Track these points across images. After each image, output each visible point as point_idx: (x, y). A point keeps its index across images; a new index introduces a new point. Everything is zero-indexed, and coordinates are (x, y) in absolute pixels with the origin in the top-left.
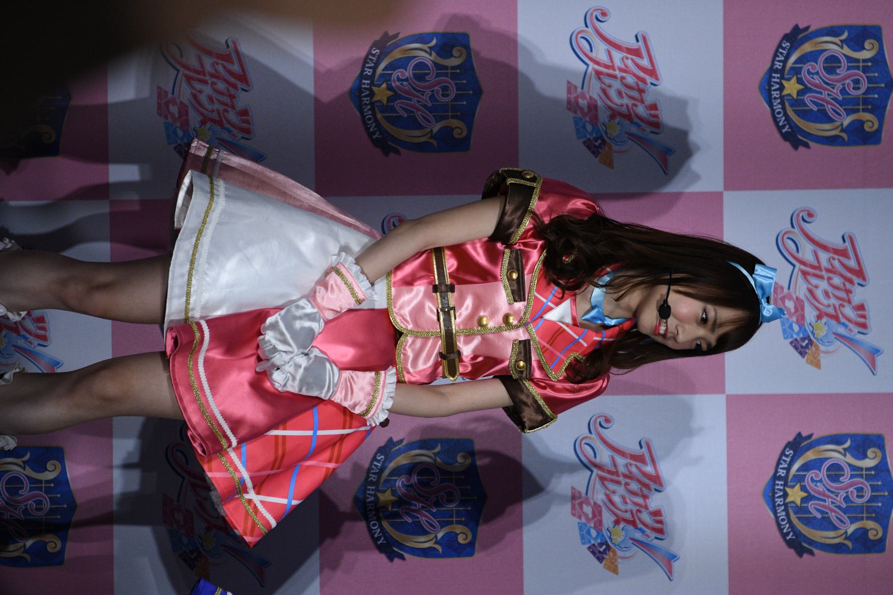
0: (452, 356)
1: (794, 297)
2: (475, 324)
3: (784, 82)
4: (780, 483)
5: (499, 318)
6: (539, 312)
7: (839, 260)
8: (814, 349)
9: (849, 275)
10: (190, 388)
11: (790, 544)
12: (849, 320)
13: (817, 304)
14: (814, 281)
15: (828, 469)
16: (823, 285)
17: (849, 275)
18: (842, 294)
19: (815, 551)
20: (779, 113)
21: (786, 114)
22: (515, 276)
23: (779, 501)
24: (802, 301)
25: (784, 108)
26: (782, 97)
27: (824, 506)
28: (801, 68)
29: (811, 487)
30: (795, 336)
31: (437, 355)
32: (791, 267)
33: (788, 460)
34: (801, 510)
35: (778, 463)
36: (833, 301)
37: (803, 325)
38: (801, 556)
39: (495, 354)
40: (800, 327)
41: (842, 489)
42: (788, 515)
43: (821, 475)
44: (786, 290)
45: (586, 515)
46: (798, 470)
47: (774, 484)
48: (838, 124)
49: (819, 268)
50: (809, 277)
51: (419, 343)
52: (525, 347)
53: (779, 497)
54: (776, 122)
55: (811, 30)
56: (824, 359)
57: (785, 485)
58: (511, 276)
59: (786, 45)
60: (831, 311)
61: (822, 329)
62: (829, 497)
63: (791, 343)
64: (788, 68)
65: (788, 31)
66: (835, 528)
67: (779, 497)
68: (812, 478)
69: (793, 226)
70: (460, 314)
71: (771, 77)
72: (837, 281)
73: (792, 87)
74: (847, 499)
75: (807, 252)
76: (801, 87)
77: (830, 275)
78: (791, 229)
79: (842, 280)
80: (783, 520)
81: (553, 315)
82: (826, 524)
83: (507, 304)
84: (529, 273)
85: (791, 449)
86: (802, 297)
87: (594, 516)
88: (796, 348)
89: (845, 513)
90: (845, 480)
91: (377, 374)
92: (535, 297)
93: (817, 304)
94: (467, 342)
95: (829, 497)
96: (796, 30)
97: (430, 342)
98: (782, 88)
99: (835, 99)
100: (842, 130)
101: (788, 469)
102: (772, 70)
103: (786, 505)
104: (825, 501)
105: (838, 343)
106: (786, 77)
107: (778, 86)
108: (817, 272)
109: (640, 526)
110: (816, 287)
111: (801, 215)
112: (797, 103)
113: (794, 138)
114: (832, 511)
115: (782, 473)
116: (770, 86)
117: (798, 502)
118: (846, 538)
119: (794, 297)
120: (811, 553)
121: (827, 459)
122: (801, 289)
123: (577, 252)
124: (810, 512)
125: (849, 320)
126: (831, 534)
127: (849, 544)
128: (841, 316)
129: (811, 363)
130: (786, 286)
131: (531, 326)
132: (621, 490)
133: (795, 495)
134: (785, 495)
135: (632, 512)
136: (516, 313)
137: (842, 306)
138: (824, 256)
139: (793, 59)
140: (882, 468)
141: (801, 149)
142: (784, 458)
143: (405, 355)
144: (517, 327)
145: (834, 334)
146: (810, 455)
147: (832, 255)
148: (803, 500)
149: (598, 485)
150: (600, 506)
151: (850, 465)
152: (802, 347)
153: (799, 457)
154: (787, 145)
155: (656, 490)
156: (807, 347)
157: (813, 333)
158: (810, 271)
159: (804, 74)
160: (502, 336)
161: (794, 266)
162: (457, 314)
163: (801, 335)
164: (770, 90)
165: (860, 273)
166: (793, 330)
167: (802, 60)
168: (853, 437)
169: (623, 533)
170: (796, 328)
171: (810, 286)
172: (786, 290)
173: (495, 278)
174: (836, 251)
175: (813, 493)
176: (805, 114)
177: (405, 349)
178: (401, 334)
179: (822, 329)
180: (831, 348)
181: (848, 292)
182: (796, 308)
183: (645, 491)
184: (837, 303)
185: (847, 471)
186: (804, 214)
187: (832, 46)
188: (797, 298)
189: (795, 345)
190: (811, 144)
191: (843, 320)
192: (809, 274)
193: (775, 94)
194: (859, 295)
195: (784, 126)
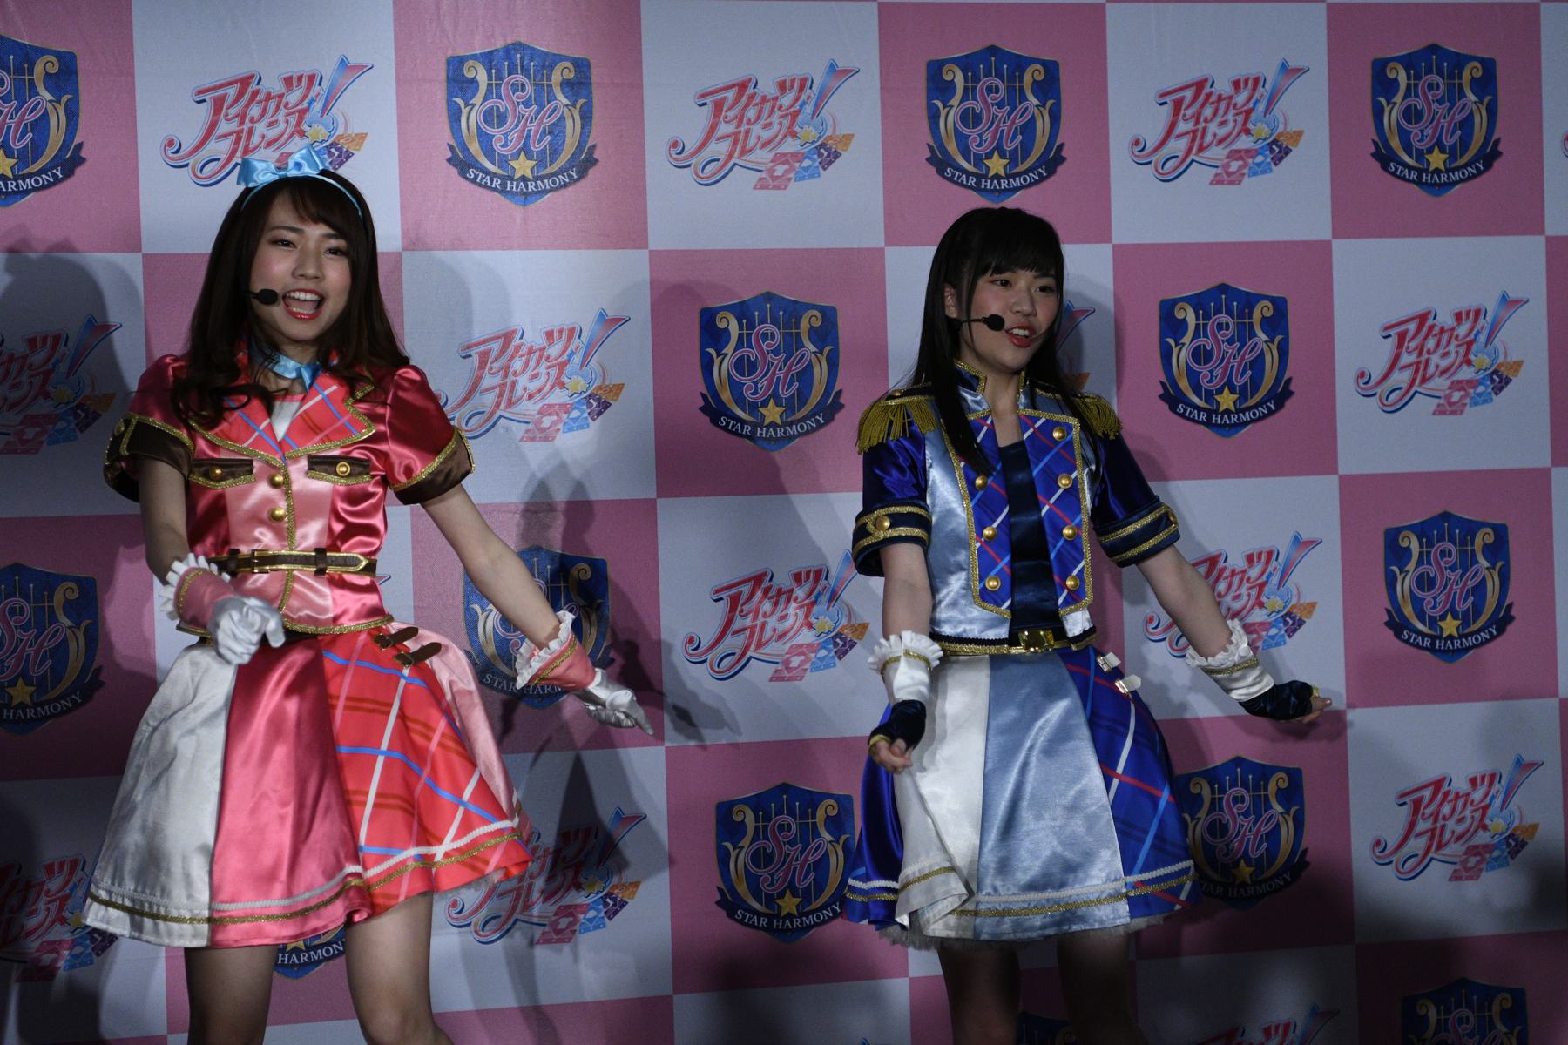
9: (744, 99)
14: (752, 141)
17: (744, 99)
21: (555, 174)
25: (548, 176)
26: (536, 179)
34: (1013, 160)
35: (961, 185)
38: (1064, 159)
42: (1019, 174)
44: (764, 175)
46: (969, 161)
47: (985, 190)
55: (452, 143)
56: (842, 130)
64: (500, 172)
65: (454, 171)
71: (511, 192)
72: (751, 113)
73: (523, 166)
74: (1000, 105)
75: (718, 149)
90: (978, 106)
99: (538, 112)
101: (968, 174)
102: (503, 191)
103: (1008, 177)
112: (541, 163)
134: (997, 177)
140: (966, 64)
164: (525, 194)
165: (742, 86)
167: (489, 153)
168: (930, 98)
172: (764, 175)
176: (555, 152)
179: (809, 132)
184: (777, 113)
186: (674, 152)
187: (472, 119)
193: (531, 187)
194: (767, 87)
195: (570, 176)
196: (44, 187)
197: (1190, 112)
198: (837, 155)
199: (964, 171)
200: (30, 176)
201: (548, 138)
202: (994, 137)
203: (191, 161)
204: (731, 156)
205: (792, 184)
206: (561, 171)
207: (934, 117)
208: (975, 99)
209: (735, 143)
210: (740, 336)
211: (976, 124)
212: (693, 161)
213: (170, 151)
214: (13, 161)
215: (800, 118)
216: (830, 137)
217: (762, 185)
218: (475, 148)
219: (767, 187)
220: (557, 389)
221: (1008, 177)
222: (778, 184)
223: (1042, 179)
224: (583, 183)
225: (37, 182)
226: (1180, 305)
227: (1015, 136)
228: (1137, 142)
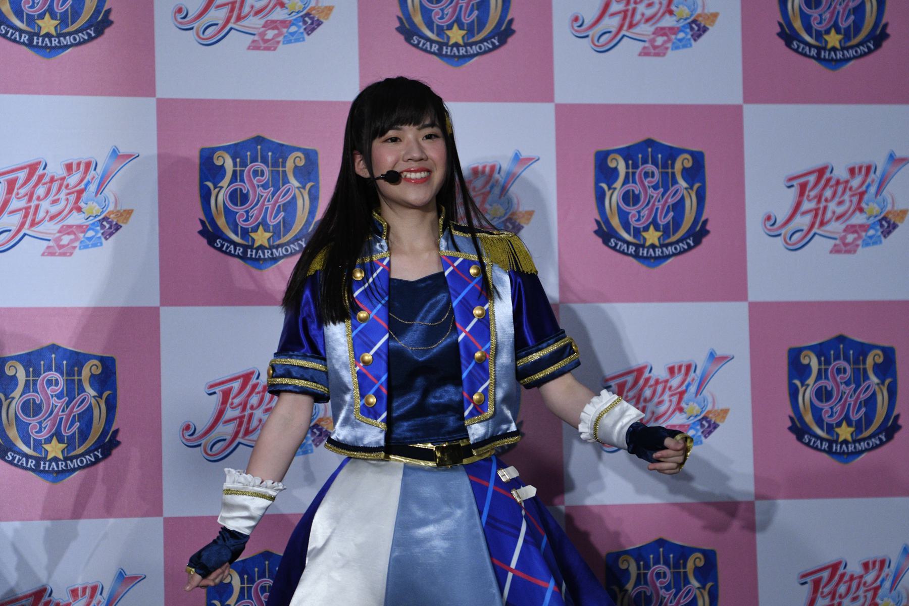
1: (652, 36)
3: (452, 42)
8: (700, 19)
13: (659, 15)
14: (638, 17)
16: (641, 8)
20: (480, 48)
24: (657, 29)
25: (476, 43)
26: (466, 45)
28: (438, 26)
30: (689, 36)
32: (625, 38)
33: (802, 46)
35: (805, 55)
44: (647, 44)
45: (855, 239)
50: (634, 22)
54: (490, 50)
56: (710, 10)
59: (415, 40)
61: (682, 10)
63: (695, 40)
69: (587, 36)
71: (446, 55)
76: (455, 27)
78: (589, 39)
80: (856, 52)
85: (792, 43)
87: (855, 232)
88: (699, 36)
93: (659, 15)
96: (401, 30)
98: (456, 45)
101: (810, 46)
106: (445, 41)
107: (455, 49)
108: (629, 14)
109: (864, 188)
110: (643, 15)
112: (471, 31)
113: (504, 33)
115: (814, 52)
116: (455, 56)
117: (840, 37)
119: (652, 36)
121: (801, 10)
129: (713, 22)
130: (642, 44)
132: (832, 206)
138: (615, 7)
139: (429, 34)
141: (514, 27)
142: (800, 50)
149: (828, 228)
150: (847, 226)
152: (699, 30)
154: (510, 40)
155: (831, 172)
158: (628, 20)
159: (444, 23)
161: (624, 36)
163: (688, 30)
166: (683, 39)
167: (430, 25)
169: (871, 204)
171: (643, 21)
172: (647, 44)
175: (832, 23)
176: (482, 22)
179: (682, 10)
183: (833, 182)
188: (654, 33)
189: (697, 36)
190: (509, 17)
195: (493, 43)
196: (80, 43)
199: (807, 44)
200: (70, 34)
201: (476, 13)
203: (196, 25)
205: (670, 53)
206: (485, 40)
209: (624, 18)
210: (627, 174)
213: (179, 16)
214: (56, 22)
217: (645, 53)
218: (418, 19)
221: (843, 49)
223: (870, 51)
225: (75, 39)
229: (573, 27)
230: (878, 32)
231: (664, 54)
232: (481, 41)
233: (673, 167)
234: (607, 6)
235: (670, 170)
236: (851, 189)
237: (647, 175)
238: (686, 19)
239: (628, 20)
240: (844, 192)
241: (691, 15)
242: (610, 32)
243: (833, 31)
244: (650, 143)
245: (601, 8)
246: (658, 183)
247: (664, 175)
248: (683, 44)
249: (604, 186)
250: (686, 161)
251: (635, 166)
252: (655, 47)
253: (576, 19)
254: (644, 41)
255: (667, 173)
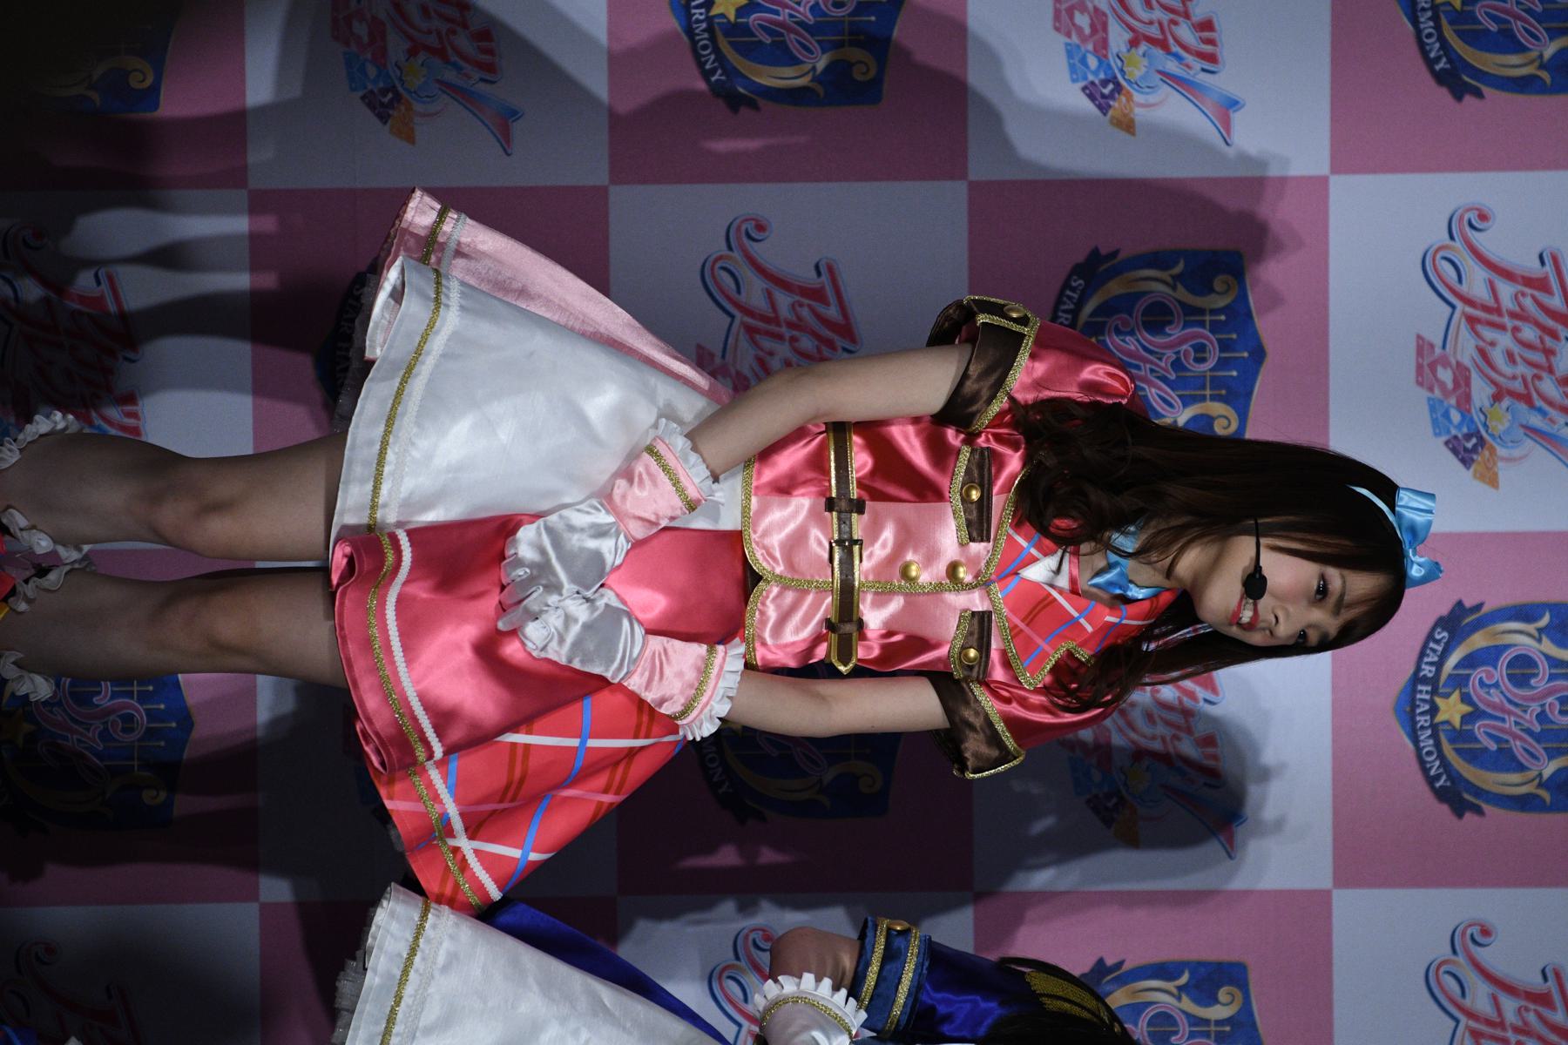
0: (849, 628)
1: (1454, 362)
2: (895, 576)
4: (1425, 688)
5: (941, 568)
6: (1010, 568)
7: (1533, 297)
8: (1486, 453)
10: (367, 644)
11: (1442, 795)
12: (1551, 403)
13: (1493, 375)
14: (1488, 334)
15: (1510, 665)
16: (1505, 340)
18: (1538, 357)
19: (1485, 807)
21: (1442, 39)
22: (975, 495)
23: (1423, 720)
25: (1438, 27)
27: (1502, 730)
29: (1479, 697)
31: (820, 623)
32: (1448, 310)
33: (1440, 648)
34: (1461, 736)
35: (1422, 654)
36: (1522, 369)
37: (1469, 411)
38: (1460, 816)
39: (928, 632)
40: (1463, 416)
41: (1533, 699)
42: (1438, 745)
43: (1497, 676)
44: (1438, 351)
46: (1456, 667)
47: (1414, 691)
48: (1534, 54)
49: (1498, 311)
50: (1479, 327)
51: (790, 597)
52: (982, 622)
53: (1422, 714)
56: (1504, 472)
57: (1434, 692)
58: (968, 495)
60: (1518, 386)
61: (1502, 420)
62: (1510, 713)
63: (1447, 443)
66: (1521, 768)
67: (1422, 714)
68: (1481, 682)
69: (1452, 237)
70: (871, 555)
72: (1529, 333)
74: (1542, 717)
75: (1477, 282)
77: (1518, 323)
78: (1448, 241)
79: (1539, 332)
80: (1429, 753)
81: (1038, 572)
82: (1505, 760)
83: (956, 545)
84: (999, 493)
85: (1444, 629)
86: (1467, 362)
88: (1455, 451)
89: (1538, 742)
90: (1540, 683)
91: (711, 651)
92: (1009, 536)
93: (1493, 375)
94: (878, 604)
95: (1510, 713)
97: (810, 598)
100: (1542, 67)
101: (1439, 665)
103: (1434, 727)
104: (1503, 720)
105: (1529, 443)
108: (1494, 318)
111: (1466, 217)
113: (1456, 80)
114: (1516, 737)
115: (1428, 671)
117: (1457, 722)
118: (1540, 785)
120: (1479, 811)
122: (1465, 348)
123: (1087, 475)
124: (1476, 740)
125: (1551, 403)
126: (1514, 778)
127: (1545, 795)
128: (1535, 395)
130: (1438, 342)
131: (995, 587)
133: (1452, 709)
134: (1434, 710)
135: (1163, 739)
136: (972, 562)
137: (1537, 377)
138: (1506, 290)
141: (1469, 100)
142: (1432, 645)
143: (762, 613)
144: (970, 587)
145: (1523, 426)
146: (1478, 641)
147: (1521, 288)
148: (1466, 719)
151: (1548, 657)
152: (1466, 450)
153: (1460, 643)
154: (1443, 94)
156: (1474, 450)
157: (1485, 425)
158: (1482, 316)
160: (943, 601)
161: (1453, 307)
162: (865, 555)
163: (1465, 430)
166: (1450, 421)
168: (1554, 608)
170: (1456, 416)
171: (1481, 344)
172: (1438, 351)
173: (937, 495)
174: (1529, 282)
177: (763, 604)
178: (758, 578)
179: (1502, 420)
180: (1516, 453)
181: (1549, 353)
182: (1456, 381)
184: (1529, 372)
185: (1544, 668)
186: (1473, 216)
189: (1454, 446)
190: (1485, 90)
191: (1538, 403)
192: (1478, 321)
195: (1438, 59)
197: (1531, 1018)
198: (1466, 462)
201: (1493, 27)
202: (1489, 704)
204: (1468, 302)
205: (1425, 393)
206: (1444, 45)
207: (1525, 613)
208: (1552, 677)
209: (1486, 309)
211: (1510, 677)
212: (1458, 244)
215: (1522, 407)
216: (1493, 451)
217: (1423, 346)
219: (1420, 352)
220: (1128, 36)
222: (1425, 370)
224: (1431, 82)
226: (1239, 995)
227: (1498, 740)
228: (1486, 932)
229: (1468, 210)
230: (1467, 796)
231: (1420, 384)
232: (1442, 39)
233: (1214, 398)
234: (1508, 275)
235: (1208, 392)
236: (1175, 737)
237: (1200, 349)
238: (1485, 425)
239: (1482, 316)
240: (1168, 723)
241: (1492, 436)
242: (1460, 280)
243: (1467, 709)
244: (1259, 354)
245: (1503, 265)
246: (1185, 369)
247: (1200, 382)
248: (1439, 421)
249: (1179, 269)
250: (1225, 422)
251: (1215, 327)
252: (1433, 367)
253: (1483, 217)
254: (1444, 347)
255: (1203, 387)
